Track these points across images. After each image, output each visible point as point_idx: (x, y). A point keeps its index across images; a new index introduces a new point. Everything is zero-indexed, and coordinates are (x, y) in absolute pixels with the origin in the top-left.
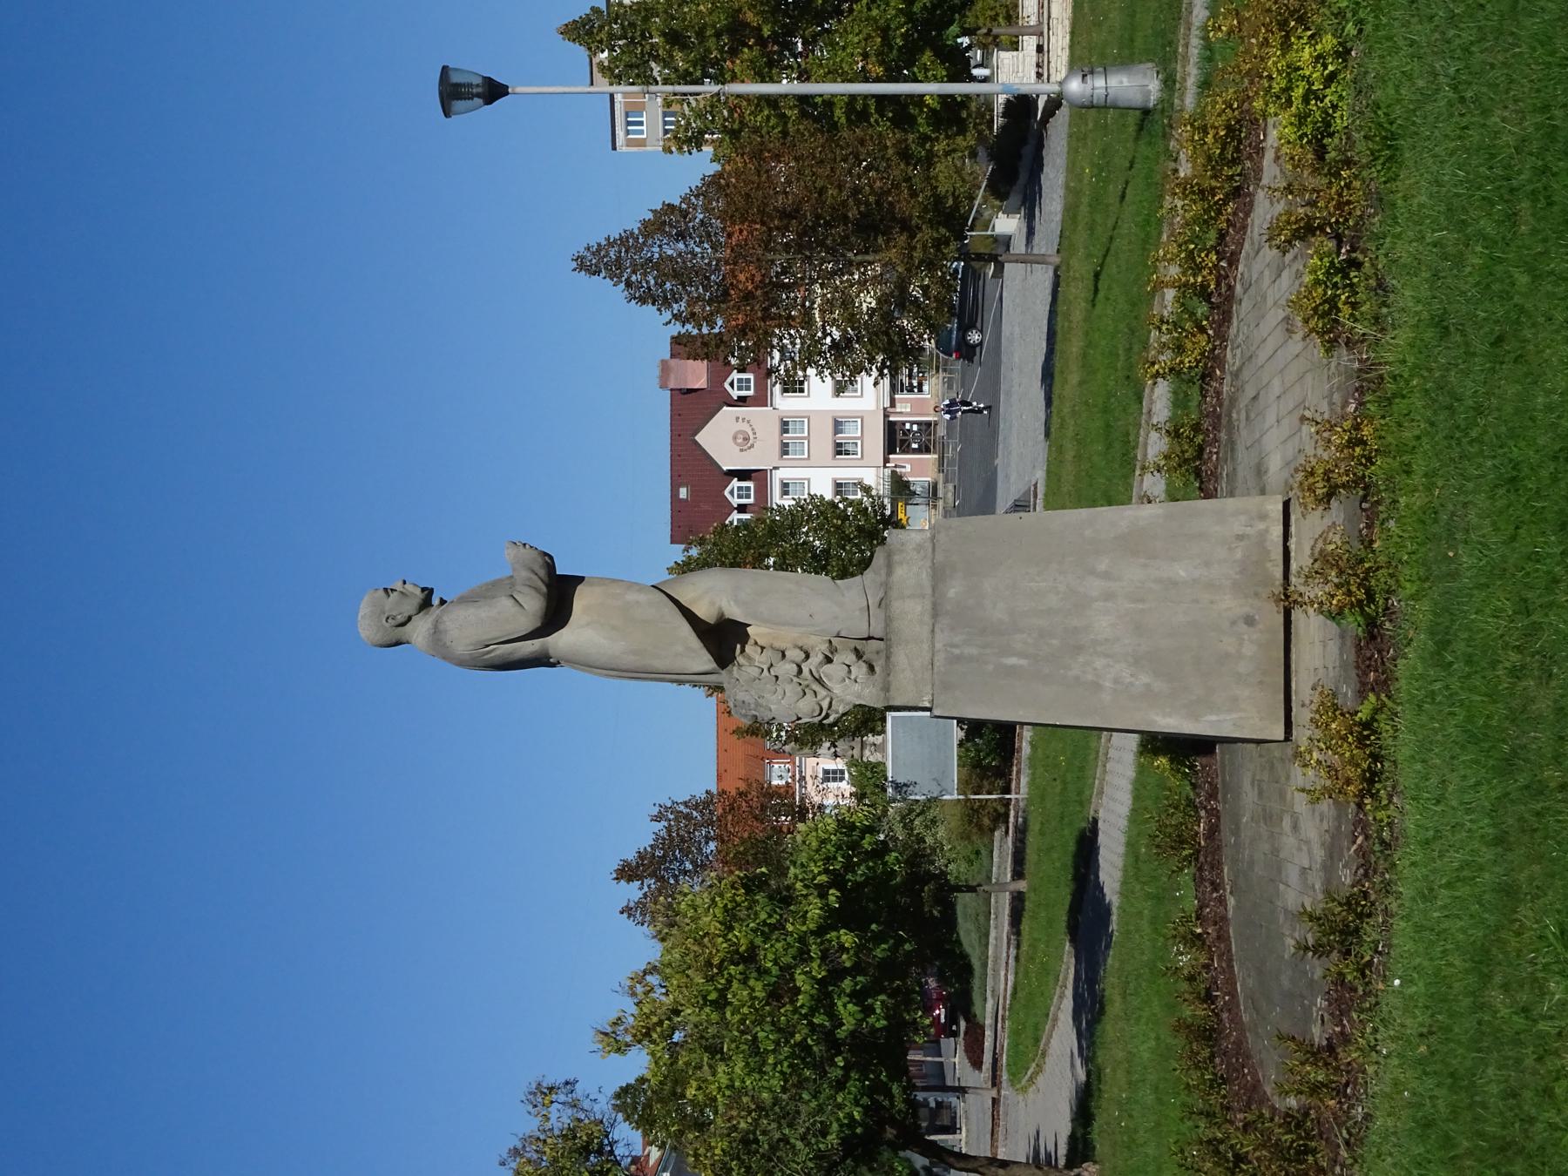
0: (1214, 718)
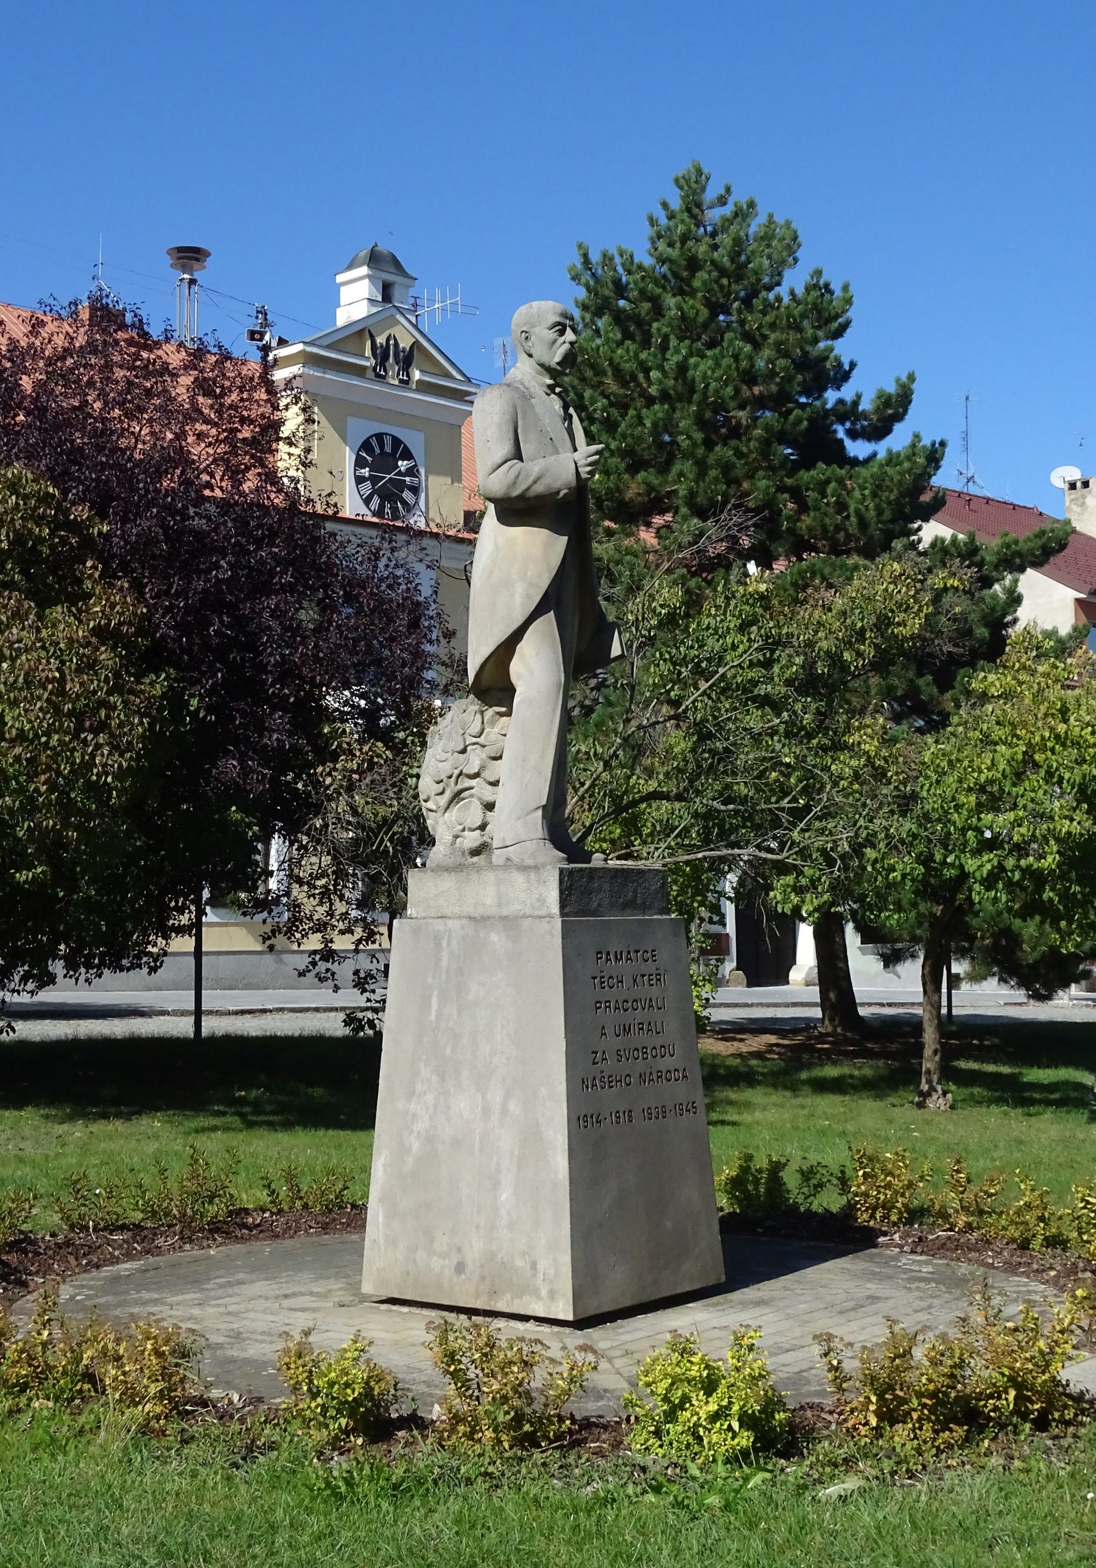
0: (381, 1219)
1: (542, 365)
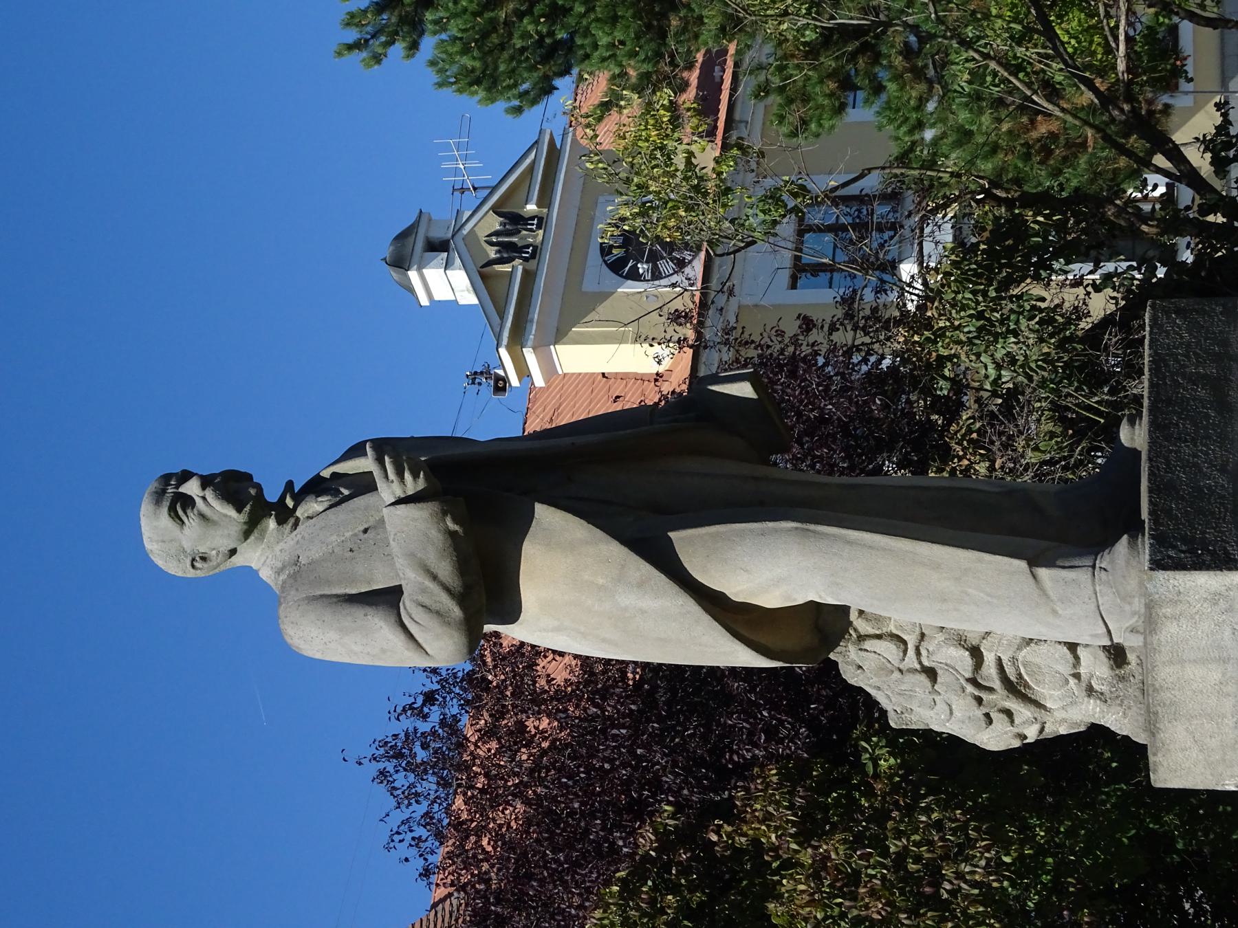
1: (247, 534)
